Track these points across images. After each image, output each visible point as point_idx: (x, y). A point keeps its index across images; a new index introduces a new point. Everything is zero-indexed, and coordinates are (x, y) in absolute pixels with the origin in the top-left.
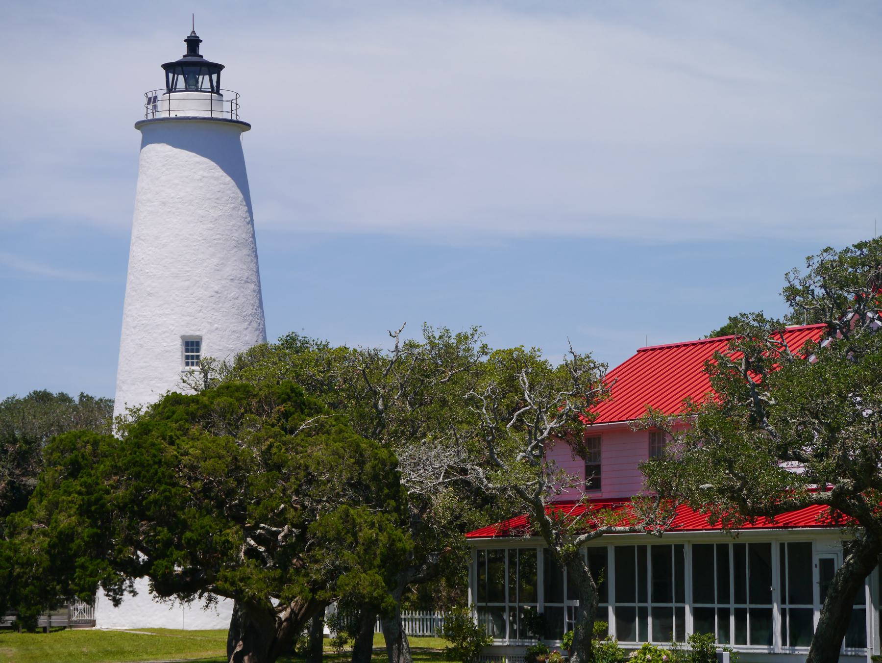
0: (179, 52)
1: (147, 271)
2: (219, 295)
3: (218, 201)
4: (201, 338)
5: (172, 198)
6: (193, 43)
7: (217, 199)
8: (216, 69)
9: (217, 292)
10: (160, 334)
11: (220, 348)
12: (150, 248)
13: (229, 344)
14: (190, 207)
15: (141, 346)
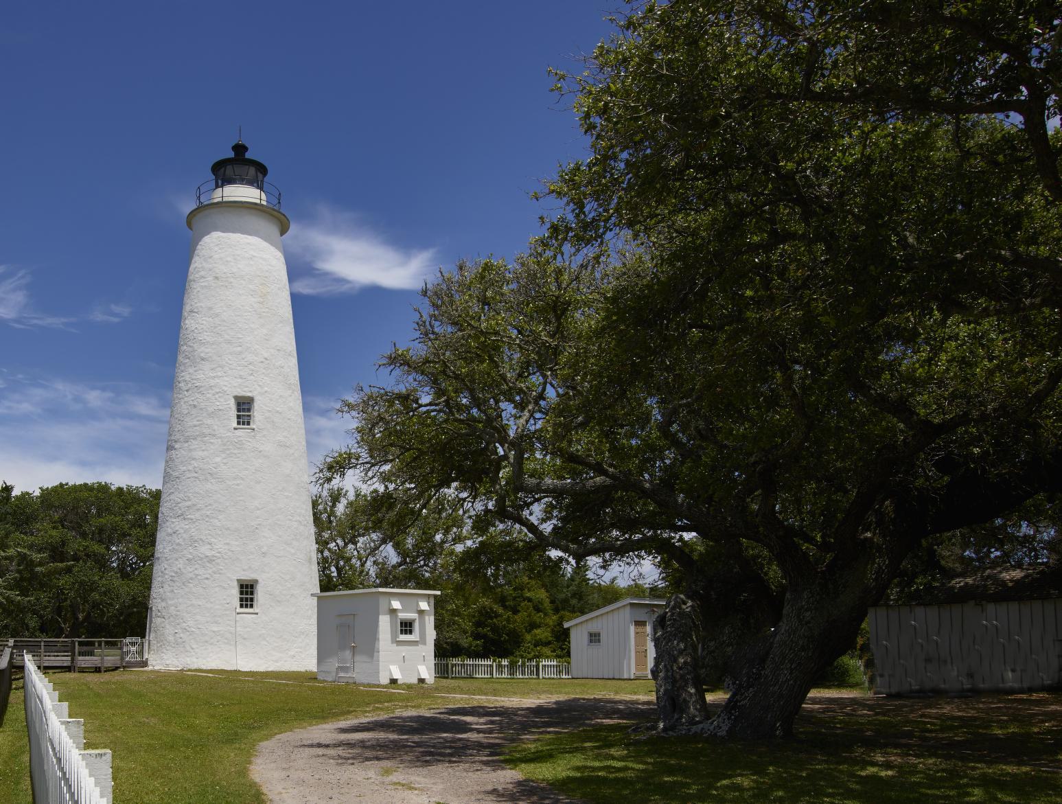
6: (240, 149)
9: (266, 359)
10: (214, 395)
15: (195, 406)
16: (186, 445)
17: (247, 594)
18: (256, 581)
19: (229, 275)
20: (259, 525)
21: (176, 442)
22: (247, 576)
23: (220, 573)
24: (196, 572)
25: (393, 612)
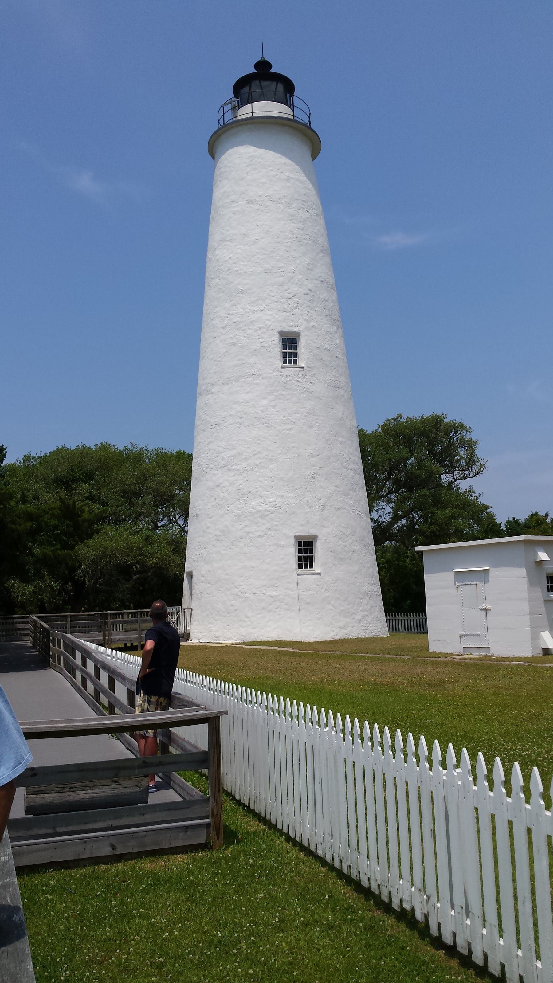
1: (237, 269)
2: (313, 294)
3: (304, 204)
4: (298, 335)
5: (260, 196)
7: (304, 201)
9: (310, 290)
11: (318, 346)
12: (238, 247)
13: (325, 344)
14: (279, 205)
15: (234, 344)
16: (226, 387)
17: (306, 552)
18: (316, 537)
19: (265, 198)
20: (315, 474)
22: (305, 532)
23: (276, 530)
24: (247, 529)
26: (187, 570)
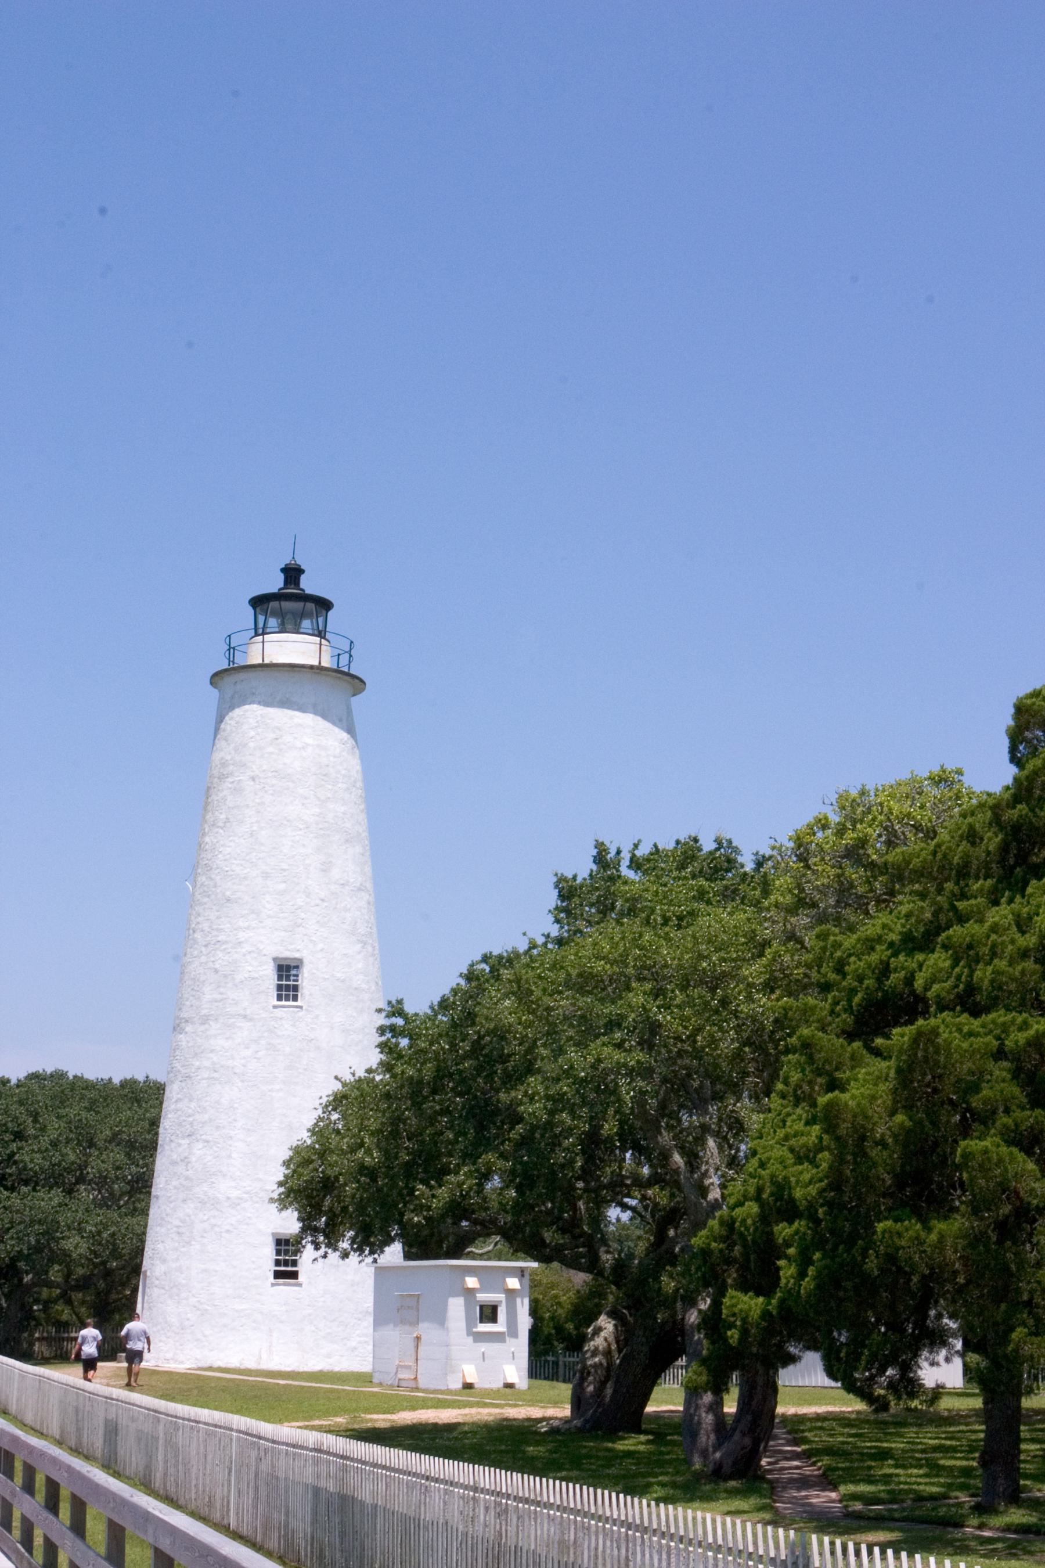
0: (275, 583)
2: (326, 904)
3: (326, 779)
6: (292, 573)
8: (324, 605)
9: (323, 900)
10: (244, 955)
16: (202, 1028)
19: (270, 774)
21: (187, 1021)
23: (248, 1224)
24: (213, 1221)
25: (470, 1292)
26: (143, 1269)
